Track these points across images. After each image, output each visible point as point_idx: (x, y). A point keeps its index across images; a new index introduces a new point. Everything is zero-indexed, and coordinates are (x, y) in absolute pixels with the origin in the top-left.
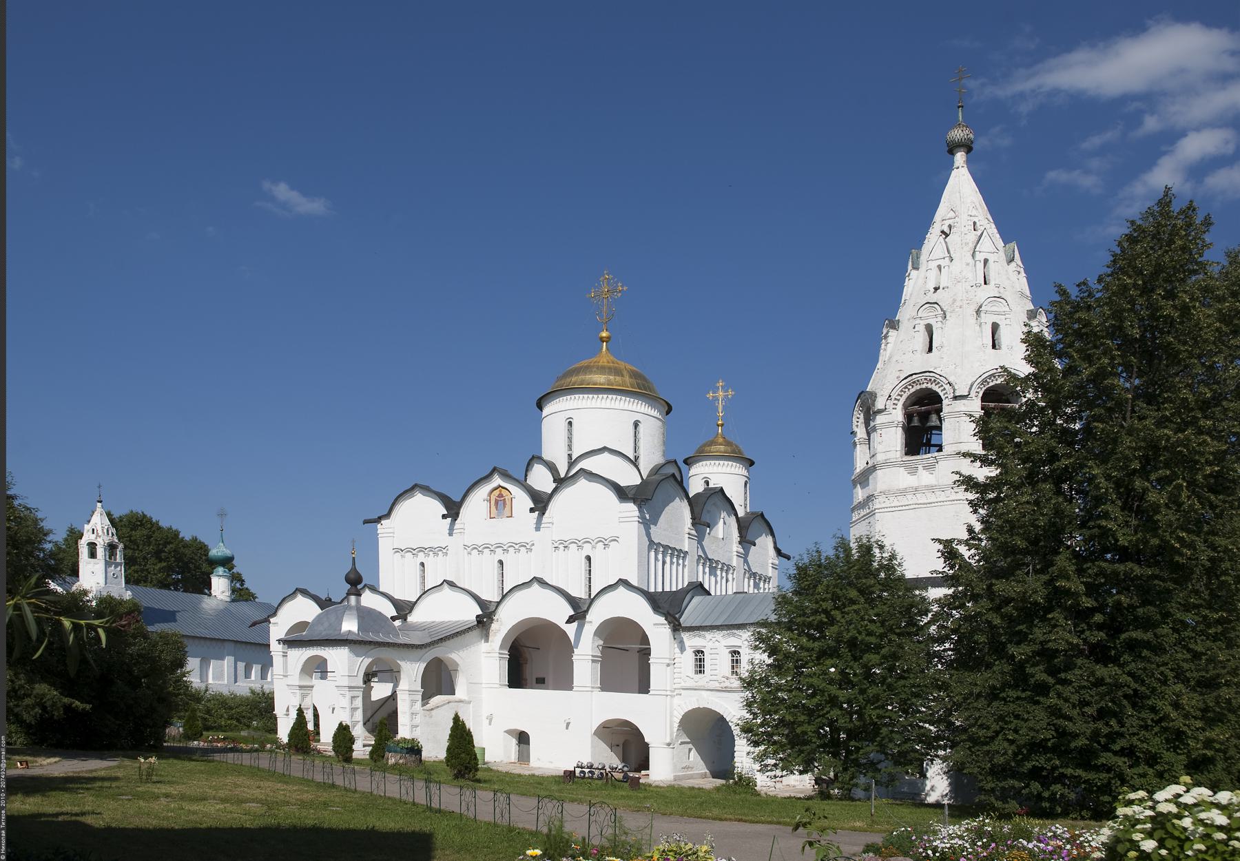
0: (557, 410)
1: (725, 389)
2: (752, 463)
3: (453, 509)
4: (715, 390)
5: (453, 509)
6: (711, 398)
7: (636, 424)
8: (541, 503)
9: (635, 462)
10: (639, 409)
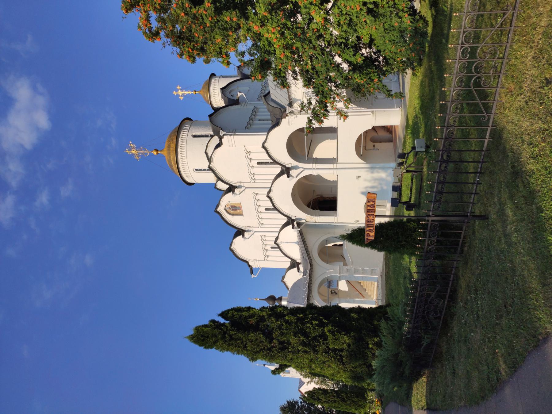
0: (191, 176)
1: (177, 91)
2: (213, 75)
3: (240, 232)
4: (178, 95)
5: (240, 232)
6: (183, 98)
7: (195, 136)
8: (231, 189)
9: (212, 136)
10: (186, 136)
